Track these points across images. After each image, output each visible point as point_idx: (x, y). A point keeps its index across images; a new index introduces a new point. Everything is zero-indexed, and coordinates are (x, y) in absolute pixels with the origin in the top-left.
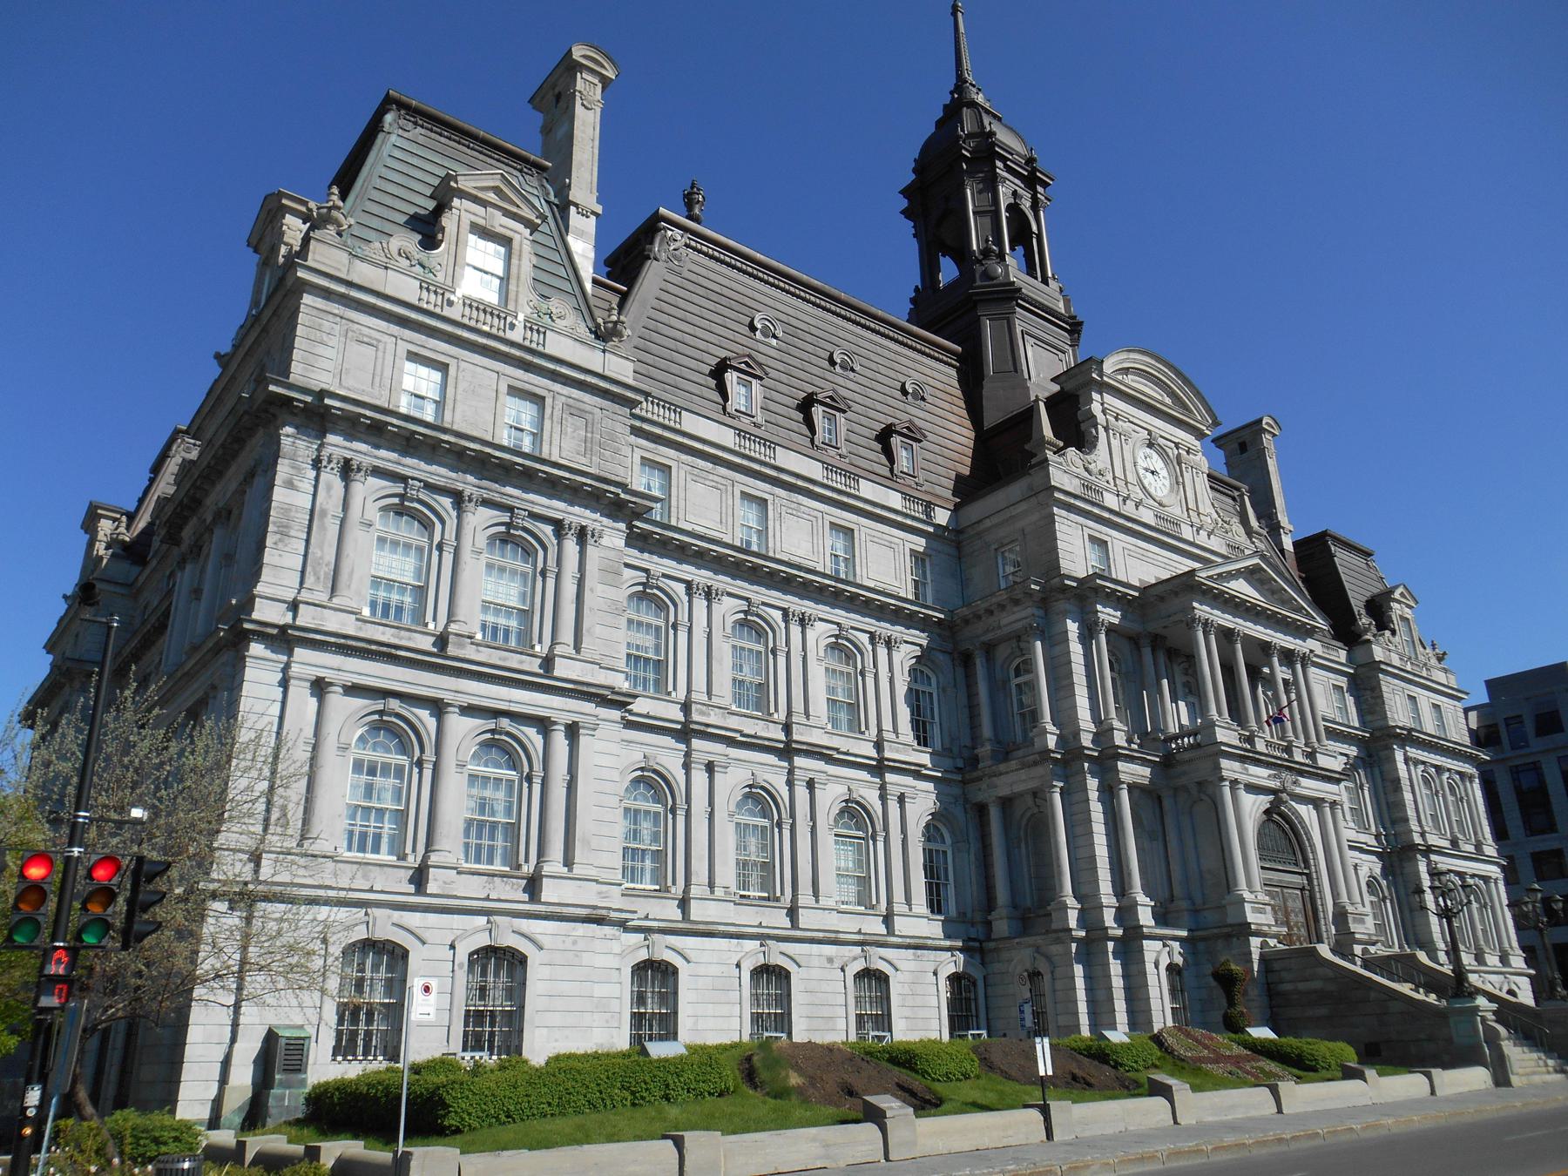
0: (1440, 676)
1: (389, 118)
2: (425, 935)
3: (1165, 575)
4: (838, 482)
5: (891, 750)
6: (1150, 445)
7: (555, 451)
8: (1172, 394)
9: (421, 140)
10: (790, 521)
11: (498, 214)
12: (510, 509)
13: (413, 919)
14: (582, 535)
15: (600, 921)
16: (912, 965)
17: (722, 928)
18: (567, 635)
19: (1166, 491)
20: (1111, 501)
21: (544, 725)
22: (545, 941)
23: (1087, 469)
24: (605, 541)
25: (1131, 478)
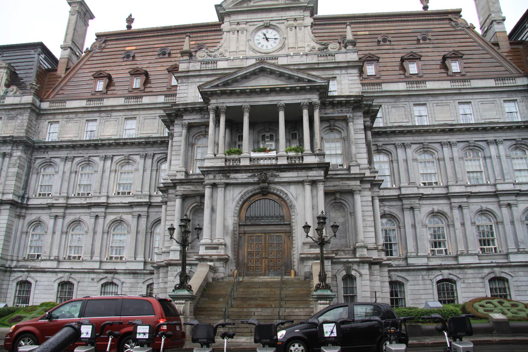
4: (132, 102)
5: (138, 198)
6: (267, 26)
10: (107, 123)
16: (132, 280)
17: (47, 270)
19: (274, 45)
23: (210, 56)
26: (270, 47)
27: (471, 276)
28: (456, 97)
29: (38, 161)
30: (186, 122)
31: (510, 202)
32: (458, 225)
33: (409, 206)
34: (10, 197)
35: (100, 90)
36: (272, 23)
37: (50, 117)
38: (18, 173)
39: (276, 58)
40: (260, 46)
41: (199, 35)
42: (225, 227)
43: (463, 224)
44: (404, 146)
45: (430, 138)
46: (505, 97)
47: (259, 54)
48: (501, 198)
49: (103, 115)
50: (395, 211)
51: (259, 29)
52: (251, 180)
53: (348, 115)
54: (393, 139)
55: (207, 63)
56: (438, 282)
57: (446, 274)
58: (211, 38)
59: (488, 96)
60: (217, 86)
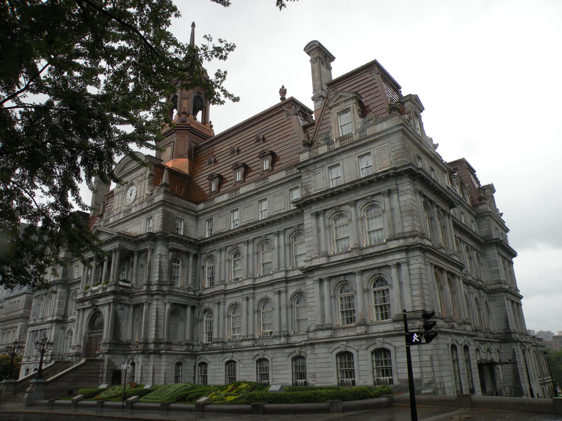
6: (132, 184)
27: (246, 358)
28: (258, 197)
29: (72, 292)
31: (281, 289)
32: (244, 314)
33: (217, 301)
34: (55, 318)
38: (59, 303)
42: (81, 334)
43: (248, 313)
44: (221, 250)
45: (237, 239)
46: (290, 185)
48: (276, 286)
50: (211, 306)
51: (128, 188)
52: (90, 305)
53: (148, 247)
54: (216, 246)
56: (227, 363)
57: (228, 357)
59: (279, 189)
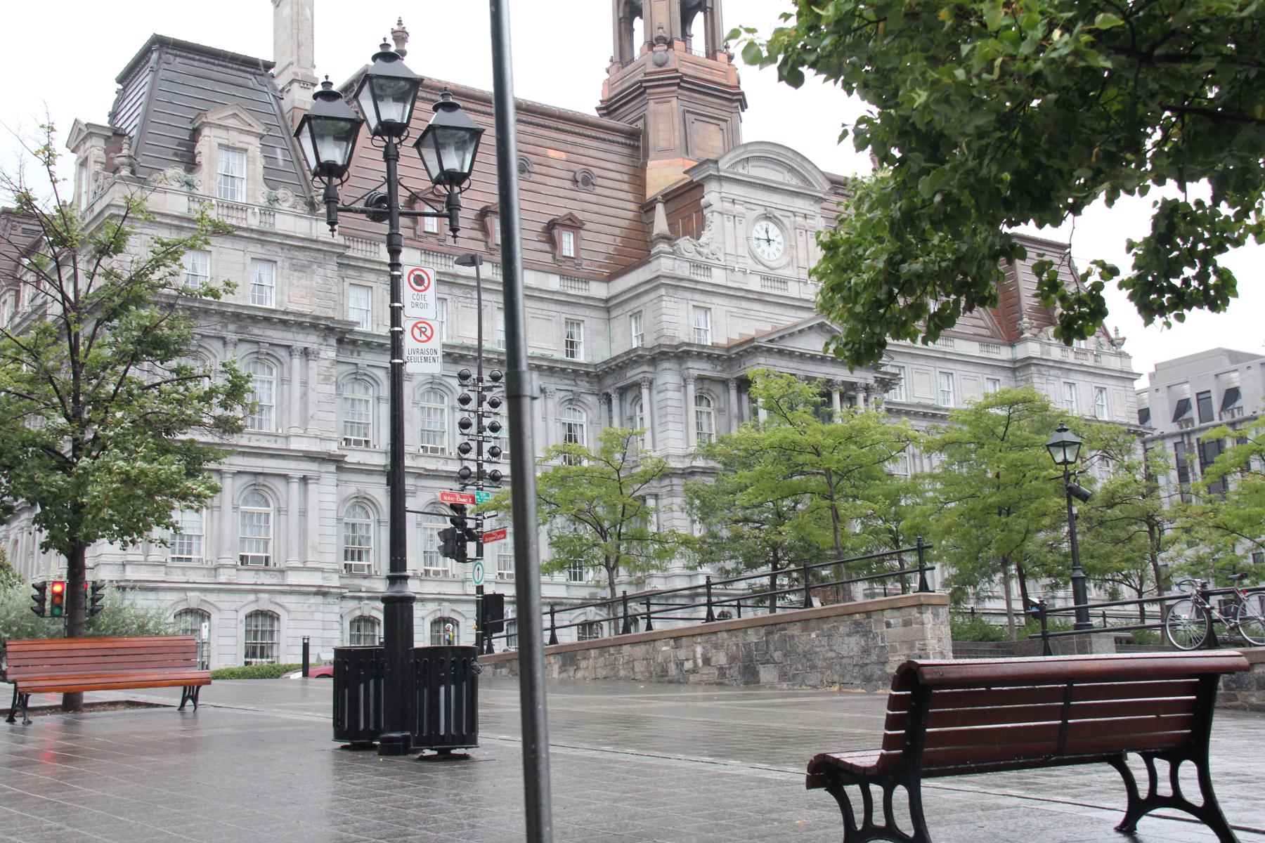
0: (1114, 363)
1: (155, 56)
2: (220, 605)
3: (768, 328)
6: (767, 218)
7: (286, 299)
8: (792, 170)
9: (180, 68)
11: (235, 133)
12: (257, 343)
13: (212, 598)
14: (306, 353)
15: (325, 594)
18: (296, 421)
19: (778, 255)
20: (718, 276)
21: (285, 477)
22: (292, 607)
23: (699, 253)
24: (323, 355)
25: (741, 251)
26: (772, 257)
28: (938, 364)
30: (696, 373)
35: (430, 230)
36: (777, 213)
37: (351, 272)
39: (784, 281)
40: (759, 250)
41: (569, 138)
47: (761, 268)
49: (457, 291)
51: (758, 219)
55: (698, 266)
58: (591, 153)
60: (771, 341)
